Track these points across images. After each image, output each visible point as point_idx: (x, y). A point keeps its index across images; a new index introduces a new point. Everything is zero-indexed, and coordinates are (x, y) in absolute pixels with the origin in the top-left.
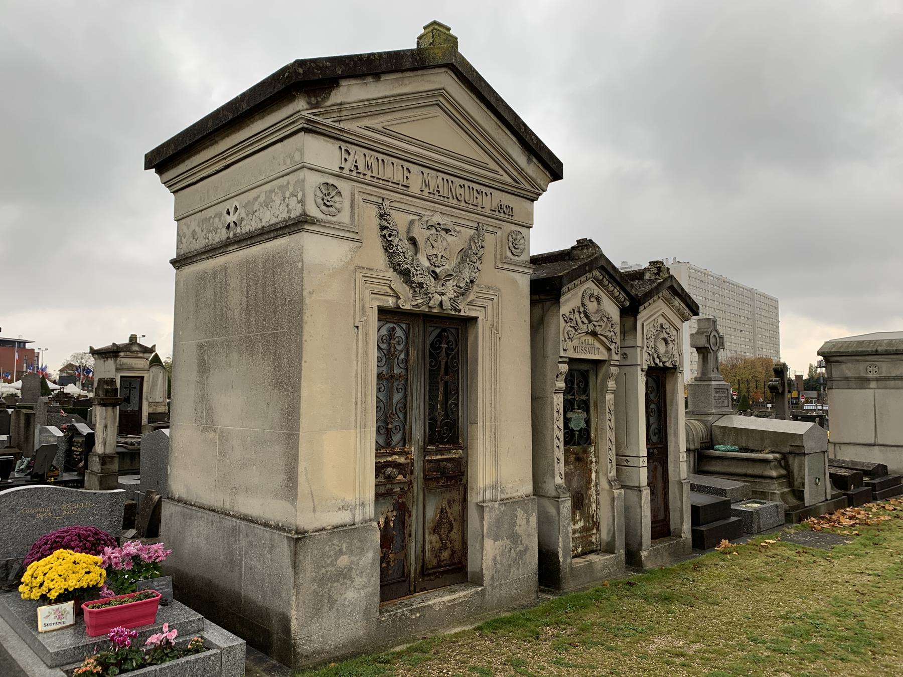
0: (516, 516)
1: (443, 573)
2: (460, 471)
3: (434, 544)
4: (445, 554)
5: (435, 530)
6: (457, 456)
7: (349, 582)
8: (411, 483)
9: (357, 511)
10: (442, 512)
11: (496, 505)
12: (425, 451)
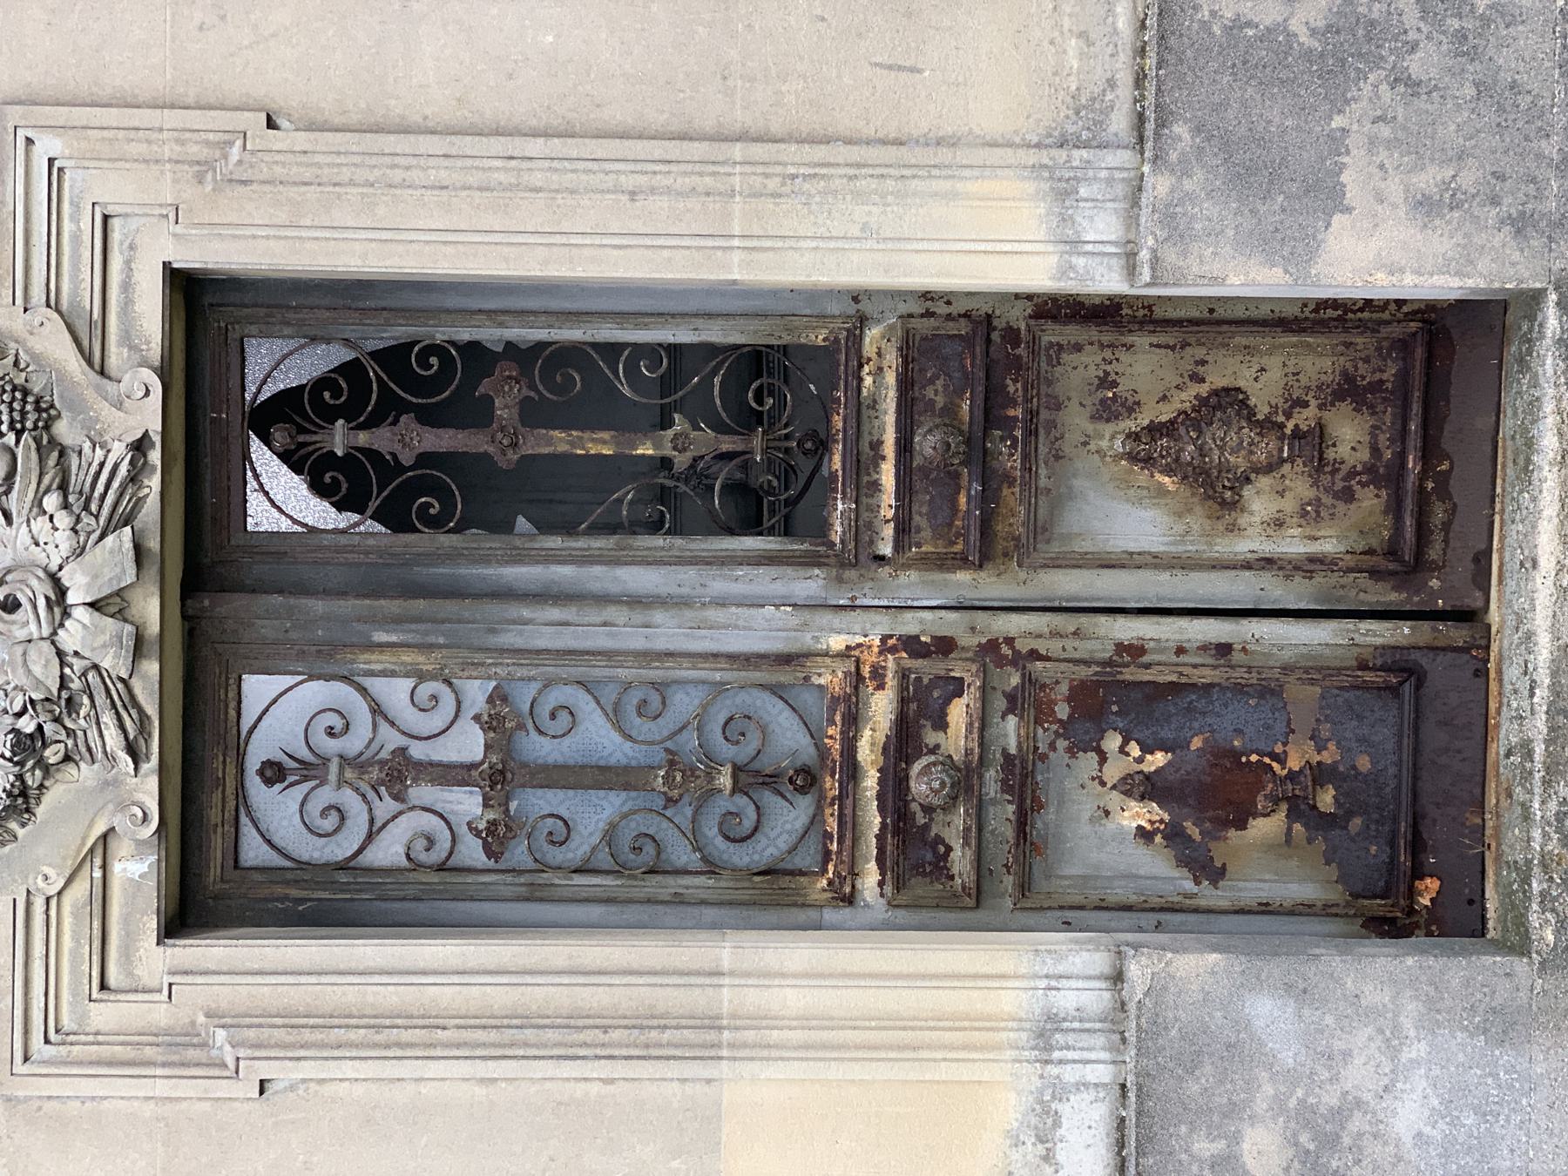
0: (1239, 24)
1: (1430, 451)
2: (967, 340)
3: (1289, 505)
4: (1349, 436)
5: (1218, 492)
6: (892, 358)
7: (1357, 1123)
8: (992, 646)
9: (1070, 1074)
10: (1147, 461)
11: (1159, 186)
12: (857, 557)
